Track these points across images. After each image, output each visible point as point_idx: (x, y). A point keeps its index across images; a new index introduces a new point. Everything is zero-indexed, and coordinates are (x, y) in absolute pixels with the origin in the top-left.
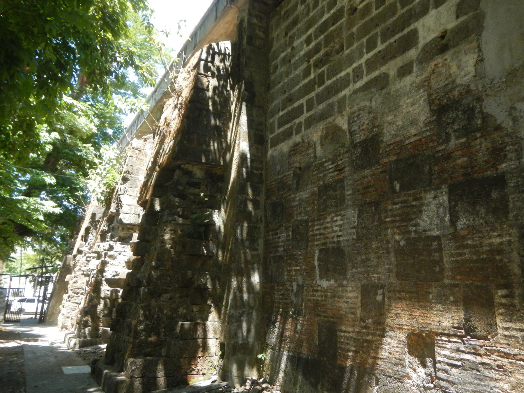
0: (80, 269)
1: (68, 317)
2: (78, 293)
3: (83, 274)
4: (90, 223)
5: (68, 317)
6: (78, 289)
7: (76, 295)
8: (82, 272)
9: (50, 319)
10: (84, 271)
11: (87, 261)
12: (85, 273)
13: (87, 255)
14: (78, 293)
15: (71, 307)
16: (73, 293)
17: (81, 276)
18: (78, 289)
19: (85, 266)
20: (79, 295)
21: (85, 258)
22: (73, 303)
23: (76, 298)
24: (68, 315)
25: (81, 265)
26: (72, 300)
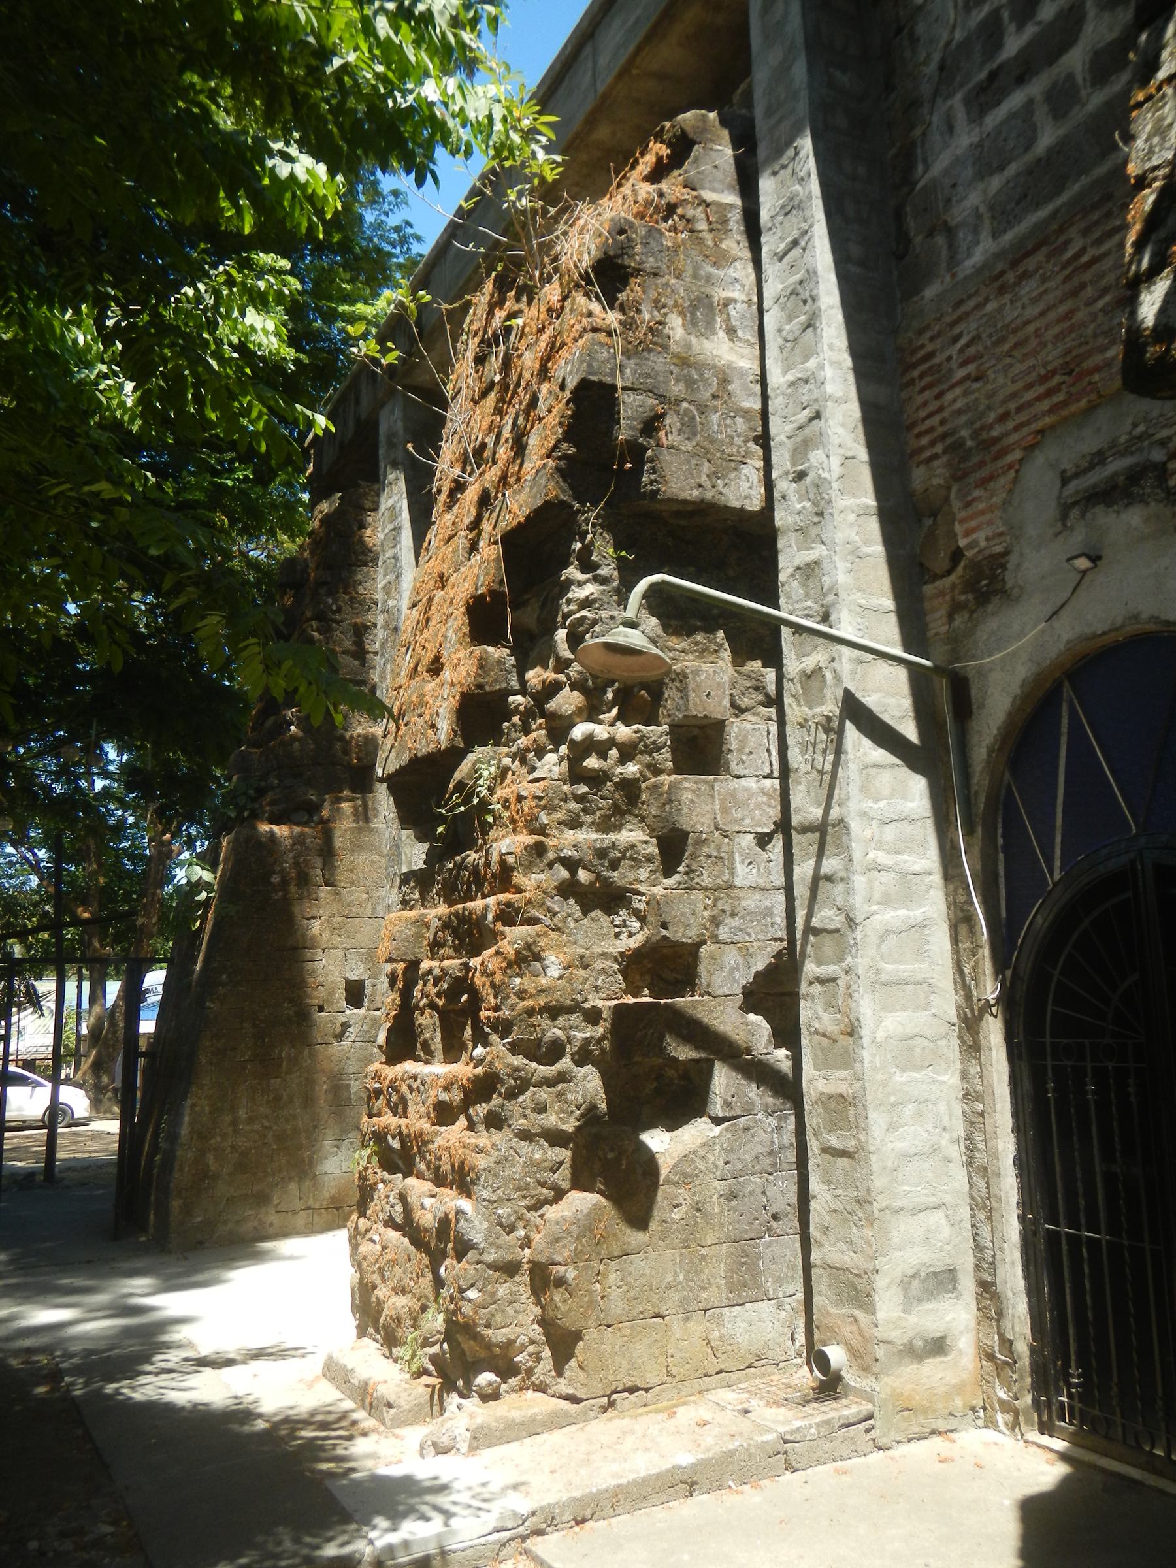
0: (539, 850)
1: (510, 1269)
2: (554, 1052)
3: (567, 889)
4: (569, 471)
5: (510, 1269)
6: (554, 1012)
7: (543, 1070)
8: (564, 874)
9: (187, 1210)
10: (572, 865)
11: (576, 775)
12: (583, 876)
13: (579, 731)
14: (554, 1052)
15: (516, 1171)
16: (514, 1049)
17: (556, 904)
18: (554, 1012)
19: (574, 823)
20: (566, 1063)
21: (551, 765)
22: (525, 1136)
23: (543, 1094)
24: (508, 1247)
25: (544, 818)
26: (519, 1113)
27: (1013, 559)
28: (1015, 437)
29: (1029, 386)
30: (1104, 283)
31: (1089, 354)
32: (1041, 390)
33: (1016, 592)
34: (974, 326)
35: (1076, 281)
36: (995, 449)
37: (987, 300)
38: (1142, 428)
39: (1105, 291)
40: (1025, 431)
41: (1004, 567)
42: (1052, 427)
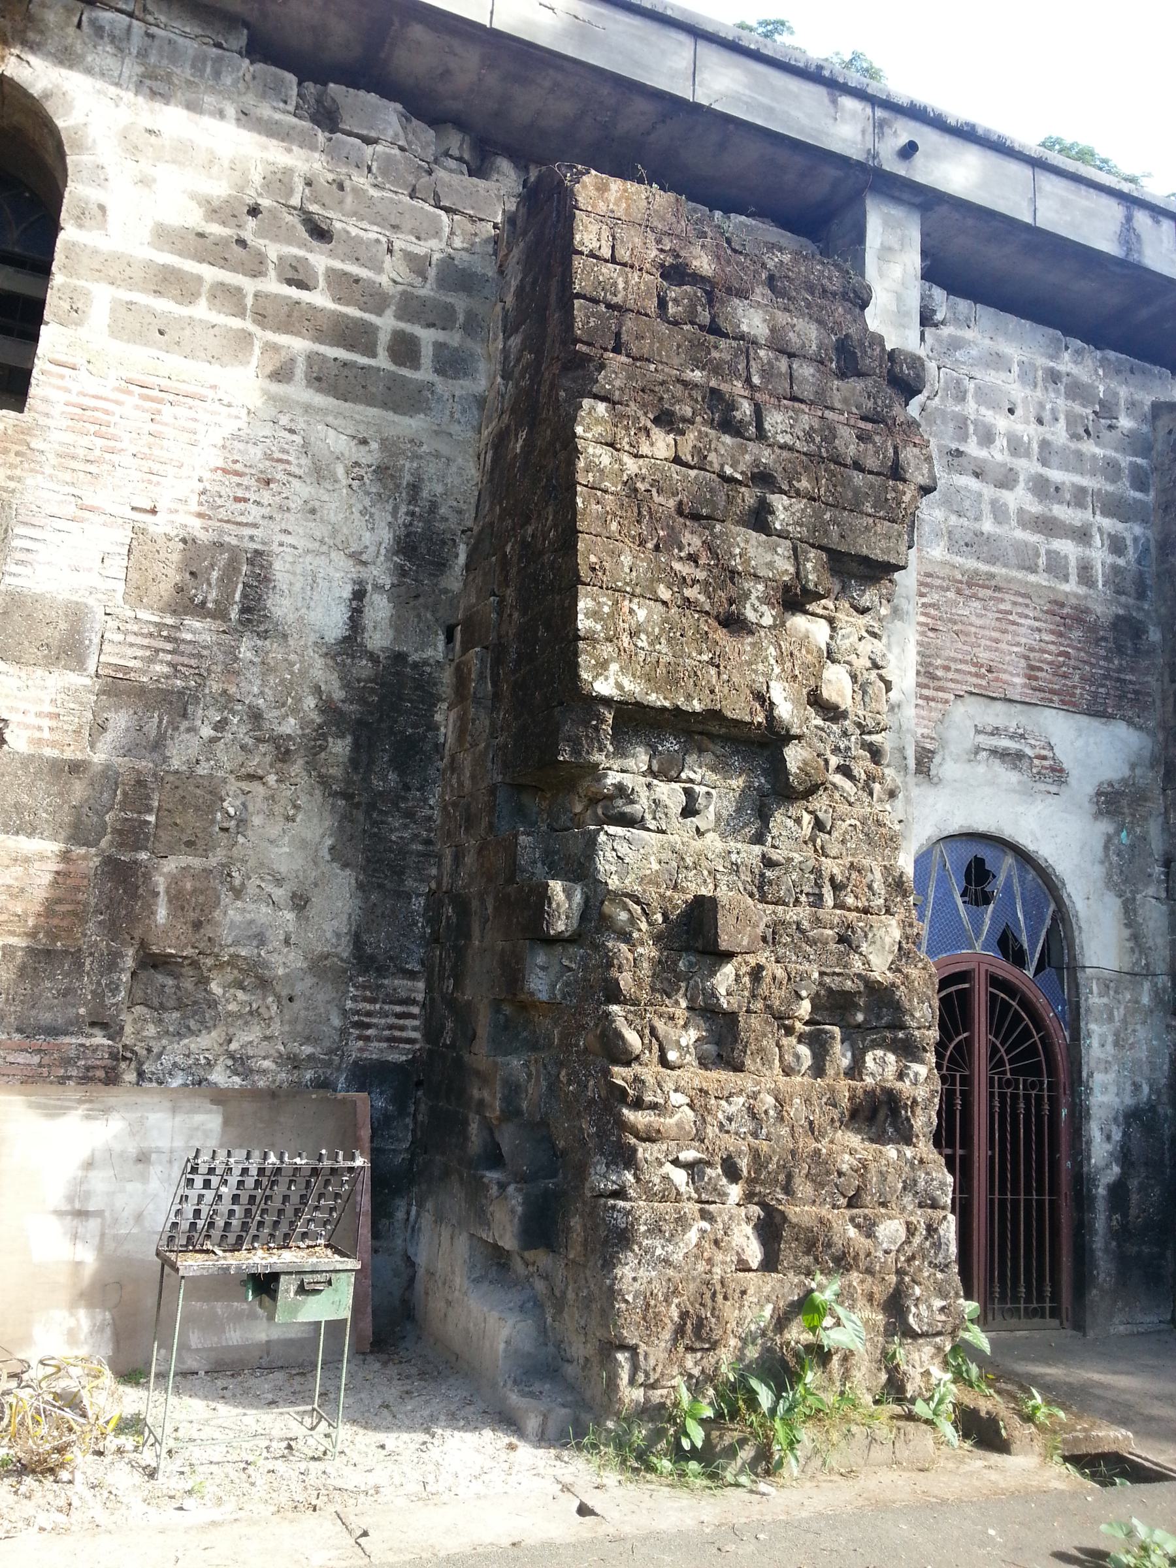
27: (937, 759)
28: (953, 685)
29: (965, 662)
30: (1017, 639)
31: (1005, 671)
32: (973, 670)
33: (936, 780)
34: (936, 597)
35: (1004, 626)
36: (937, 683)
37: (948, 589)
38: (1021, 731)
39: (1018, 644)
40: (959, 686)
41: (931, 760)
42: (971, 693)
